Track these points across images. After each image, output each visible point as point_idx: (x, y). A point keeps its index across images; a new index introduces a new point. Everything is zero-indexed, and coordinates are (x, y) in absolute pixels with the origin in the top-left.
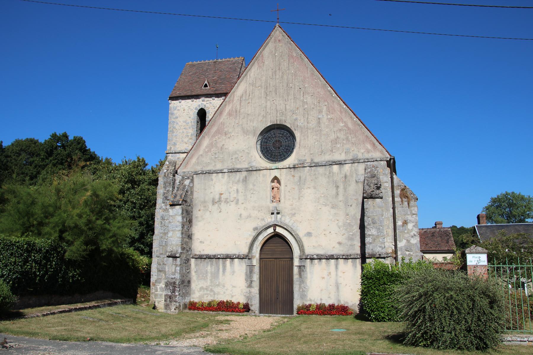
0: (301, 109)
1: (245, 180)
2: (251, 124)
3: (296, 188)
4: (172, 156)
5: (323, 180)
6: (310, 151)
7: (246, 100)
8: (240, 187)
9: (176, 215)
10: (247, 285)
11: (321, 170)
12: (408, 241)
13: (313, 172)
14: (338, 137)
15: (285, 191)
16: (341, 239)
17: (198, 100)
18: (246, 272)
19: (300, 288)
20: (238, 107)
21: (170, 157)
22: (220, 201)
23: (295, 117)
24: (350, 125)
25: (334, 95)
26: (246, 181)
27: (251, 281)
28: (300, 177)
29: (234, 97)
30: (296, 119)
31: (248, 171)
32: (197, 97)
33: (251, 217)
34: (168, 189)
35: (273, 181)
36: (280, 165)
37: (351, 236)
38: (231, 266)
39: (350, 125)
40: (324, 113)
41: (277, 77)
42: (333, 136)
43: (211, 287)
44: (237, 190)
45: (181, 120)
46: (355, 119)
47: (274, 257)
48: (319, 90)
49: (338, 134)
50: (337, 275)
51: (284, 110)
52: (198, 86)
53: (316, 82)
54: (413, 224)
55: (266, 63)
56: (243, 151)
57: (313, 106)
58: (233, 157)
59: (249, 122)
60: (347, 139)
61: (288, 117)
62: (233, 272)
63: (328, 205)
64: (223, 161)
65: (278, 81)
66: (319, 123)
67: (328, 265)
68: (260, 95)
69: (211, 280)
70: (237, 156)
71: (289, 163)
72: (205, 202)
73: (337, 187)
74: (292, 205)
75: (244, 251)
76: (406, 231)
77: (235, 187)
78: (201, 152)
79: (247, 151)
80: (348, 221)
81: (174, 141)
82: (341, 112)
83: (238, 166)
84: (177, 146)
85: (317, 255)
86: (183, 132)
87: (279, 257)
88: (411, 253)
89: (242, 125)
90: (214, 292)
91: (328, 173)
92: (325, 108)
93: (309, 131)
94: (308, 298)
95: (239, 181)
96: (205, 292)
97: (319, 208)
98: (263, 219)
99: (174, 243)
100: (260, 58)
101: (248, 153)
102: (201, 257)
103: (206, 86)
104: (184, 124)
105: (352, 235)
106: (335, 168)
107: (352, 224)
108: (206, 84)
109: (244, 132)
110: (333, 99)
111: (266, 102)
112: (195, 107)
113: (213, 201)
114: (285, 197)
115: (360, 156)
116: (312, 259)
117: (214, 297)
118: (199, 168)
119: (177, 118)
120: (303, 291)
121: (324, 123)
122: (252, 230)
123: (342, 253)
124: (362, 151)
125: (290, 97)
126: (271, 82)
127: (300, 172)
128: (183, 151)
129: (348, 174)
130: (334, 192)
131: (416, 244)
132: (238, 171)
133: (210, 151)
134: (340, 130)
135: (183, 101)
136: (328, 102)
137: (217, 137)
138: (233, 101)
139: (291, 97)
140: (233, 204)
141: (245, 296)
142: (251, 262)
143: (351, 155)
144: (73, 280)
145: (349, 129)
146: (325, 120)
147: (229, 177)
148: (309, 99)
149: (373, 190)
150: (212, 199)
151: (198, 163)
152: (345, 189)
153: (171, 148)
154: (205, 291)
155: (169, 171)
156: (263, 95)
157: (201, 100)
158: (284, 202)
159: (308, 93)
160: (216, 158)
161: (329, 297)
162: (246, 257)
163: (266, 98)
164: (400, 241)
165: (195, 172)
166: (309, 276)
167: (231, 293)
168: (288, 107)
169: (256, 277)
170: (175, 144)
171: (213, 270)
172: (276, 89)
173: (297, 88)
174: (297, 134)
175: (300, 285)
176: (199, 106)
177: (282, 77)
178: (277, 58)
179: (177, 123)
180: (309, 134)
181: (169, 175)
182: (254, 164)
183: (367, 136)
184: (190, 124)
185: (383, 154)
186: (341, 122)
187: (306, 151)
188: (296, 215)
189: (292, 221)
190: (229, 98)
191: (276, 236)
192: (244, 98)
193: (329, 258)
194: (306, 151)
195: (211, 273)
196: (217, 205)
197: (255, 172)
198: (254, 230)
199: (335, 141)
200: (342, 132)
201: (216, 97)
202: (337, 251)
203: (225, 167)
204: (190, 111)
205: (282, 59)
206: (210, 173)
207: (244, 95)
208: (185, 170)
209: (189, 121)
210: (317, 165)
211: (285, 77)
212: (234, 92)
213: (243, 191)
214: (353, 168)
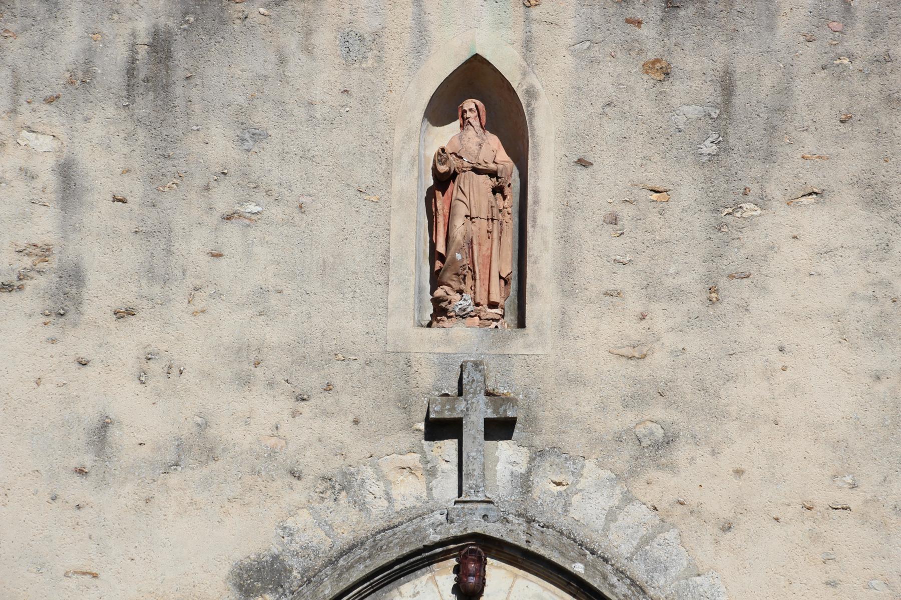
3: (688, 189)
8: (102, 142)
15: (567, 211)
28: (727, 86)
33: (210, 454)
35: (443, 108)
44: (67, 174)
77: (44, 143)
95: (83, 79)
98: (340, 484)
114: (567, 270)
127: (732, 35)
158: (563, 323)
188: (681, 453)
189: (638, 512)
213: (134, 188)
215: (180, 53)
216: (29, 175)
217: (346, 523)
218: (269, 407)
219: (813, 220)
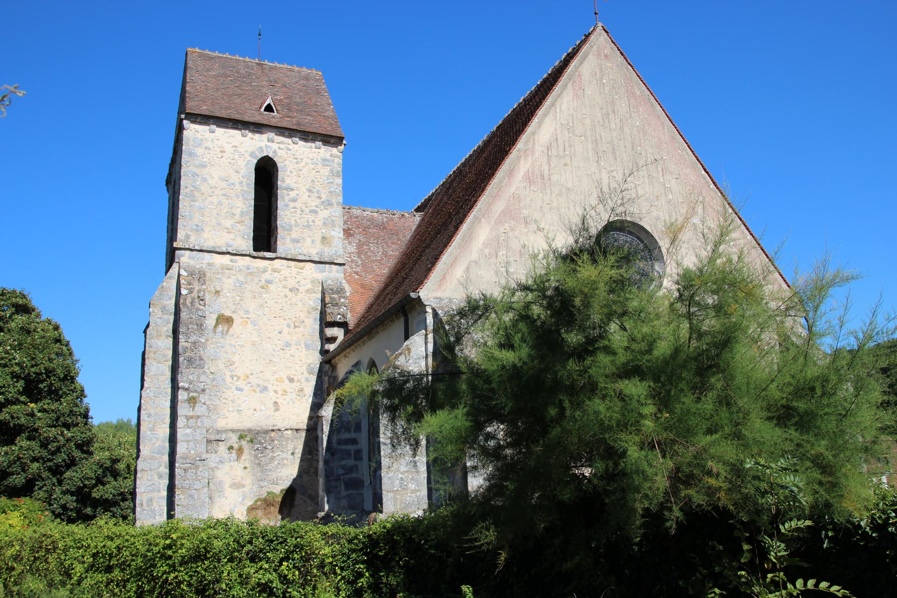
4: (190, 258)
17: (257, 136)
20: (545, 167)
25: (712, 186)
29: (534, 144)
32: (257, 127)
41: (613, 126)
55: (588, 92)
68: (585, 154)
78: (474, 255)
84: (206, 235)
104: (224, 184)
111: (600, 172)
112: (250, 150)
119: (205, 166)
126: (603, 134)
128: (224, 250)
135: (220, 131)
137: (507, 226)
138: (533, 152)
153: (188, 237)
156: (591, 155)
157: (265, 137)
159: (671, 173)
163: (597, 162)
170: (199, 230)
177: (621, 129)
178: (607, 89)
179: (205, 180)
201: (301, 139)
204: (237, 157)
207: (554, 145)
208: (439, 294)
209: (235, 178)
211: (627, 130)
212: (534, 133)
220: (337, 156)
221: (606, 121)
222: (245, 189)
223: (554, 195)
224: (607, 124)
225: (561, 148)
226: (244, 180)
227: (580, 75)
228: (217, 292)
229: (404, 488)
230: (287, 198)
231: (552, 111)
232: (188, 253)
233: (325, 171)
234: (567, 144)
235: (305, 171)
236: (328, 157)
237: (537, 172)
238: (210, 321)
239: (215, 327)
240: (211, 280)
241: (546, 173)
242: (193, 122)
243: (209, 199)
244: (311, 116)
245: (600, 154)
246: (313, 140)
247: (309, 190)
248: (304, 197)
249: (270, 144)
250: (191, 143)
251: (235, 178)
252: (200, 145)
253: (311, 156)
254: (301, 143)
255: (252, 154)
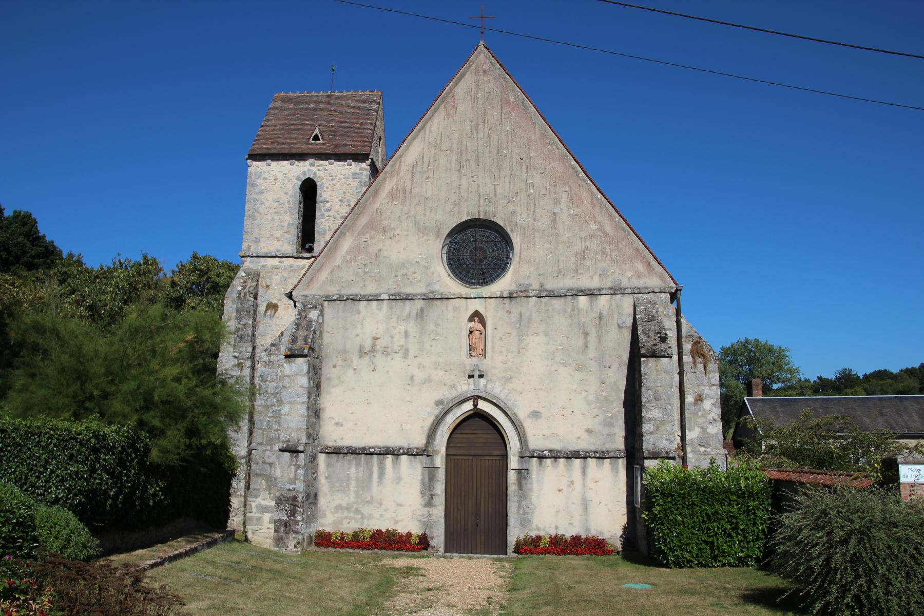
0: (522, 196)
1: (421, 315)
2: (432, 215)
3: (514, 333)
5: (562, 322)
6: (537, 268)
7: (422, 172)
9: (297, 374)
10: (423, 503)
11: (557, 303)
12: (704, 430)
13: (543, 307)
14: (587, 248)
15: (493, 337)
16: (591, 423)
17: (302, 163)
18: (422, 480)
19: (519, 507)
20: (408, 183)
21: (248, 263)
22: (373, 350)
23: (511, 208)
24: (608, 229)
25: (582, 174)
26: (422, 317)
27: (432, 496)
28: (521, 315)
29: (400, 165)
30: (513, 213)
31: (427, 298)
32: (301, 157)
33: (430, 381)
34: (244, 321)
35: (471, 319)
36: (485, 291)
37: (609, 420)
38: (394, 467)
39: (608, 229)
40: (563, 205)
41: (481, 135)
42: (578, 246)
43: (355, 506)
45: (269, 198)
46: (618, 219)
47: (472, 452)
48: (556, 164)
49: (588, 244)
50: (584, 485)
51: (492, 195)
52: (300, 138)
53: (549, 150)
54: (712, 401)
56: (418, 262)
57: (544, 192)
58: (399, 274)
59: (428, 212)
60: (603, 252)
61: (500, 208)
62: (398, 479)
63: (570, 365)
64: (378, 279)
65: (481, 142)
66: (554, 221)
67: (569, 468)
68: (448, 166)
69: (356, 492)
70: (405, 271)
71: (500, 289)
72: (344, 351)
73: (586, 334)
74: (505, 363)
75: (419, 441)
76: (700, 413)
77: (402, 327)
78: (338, 261)
79: (424, 263)
80: (604, 394)
81: (255, 235)
82: (593, 206)
83: (408, 290)
84: (262, 244)
85: (550, 451)
86: (273, 220)
87: (480, 452)
88: (709, 450)
89: (415, 217)
90: (362, 514)
91: (569, 310)
92: (565, 196)
93: (537, 234)
94: (534, 526)
95: (409, 316)
96: (346, 514)
97: (553, 369)
98: (453, 386)
99: (293, 425)
100: (449, 100)
101: (427, 268)
102: (337, 452)
103: (316, 138)
104: (276, 204)
105: (611, 417)
106: (583, 301)
107: (611, 398)
108: (316, 135)
109: (419, 230)
110: (580, 182)
111: (460, 179)
113: (360, 351)
114: (493, 348)
115: (625, 283)
116: (541, 458)
117: (362, 523)
118: (333, 290)
119: (263, 193)
120: (525, 513)
121: (564, 223)
122: (432, 404)
123: (593, 448)
124: (629, 274)
125: (503, 173)
126: (469, 145)
128: (274, 254)
129: (605, 313)
130: (580, 343)
131: (716, 434)
132: (408, 298)
133: (354, 259)
134: (592, 236)
135: (274, 164)
136: (569, 186)
137: (367, 236)
139: (505, 172)
140: (398, 358)
141: (420, 521)
142: (432, 461)
143: (610, 279)
144: (154, 502)
145: (606, 234)
146: (564, 216)
147: (391, 308)
148: (537, 179)
149: (655, 342)
150: (357, 348)
151: (331, 281)
152: (599, 338)
153: (249, 247)
154: (346, 511)
155: (247, 290)
156: (453, 165)
157: (307, 163)
158: (492, 358)
159: (536, 169)
160: (365, 273)
161: (571, 524)
162: (425, 452)
163: (459, 171)
164: (690, 430)
165: (326, 297)
166: (535, 486)
167: (394, 515)
168: (499, 190)
169: (440, 488)
170: (257, 241)
171: (361, 475)
172: (478, 156)
173: (516, 158)
174: (516, 239)
175: (519, 502)
176: (304, 173)
177: (489, 136)
178: (480, 102)
179: (262, 203)
180: (537, 240)
181: (248, 297)
182: (437, 287)
183: (637, 250)
184: (286, 205)
185: (665, 282)
186: (592, 223)
187: (532, 269)
188: (513, 380)
189: (506, 391)
190: (392, 166)
191: (478, 415)
192: (419, 169)
193: (572, 455)
194: (532, 269)
195: (357, 480)
196: (367, 358)
197: (439, 303)
198: (437, 405)
199: (583, 254)
200: (594, 240)
202: (584, 444)
203: (383, 291)
204: (286, 182)
205: (490, 104)
206: (354, 299)
207: (420, 163)
209: (285, 199)
210: (551, 295)
212: (401, 156)
213: (417, 335)
214: (613, 302)
215: (425, 311)
216: (400, 333)
217: (454, 393)
218: (441, 373)
219: (536, 339)
220: (365, 169)
221: (475, 132)
222: (292, 205)
223: (412, 205)
224: (475, 135)
225: (426, 164)
226: (291, 199)
227: (454, 96)
228: (268, 286)
229: (270, 428)
230: (323, 209)
231: (421, 134)
232: (249, 259)
233: (355, 183)
234: (432, 160)
235: (338, 185)
236: (358, 171)
237: (400, 188)
238: (262, 308)
239: (266, 312)
240: (263, 278)
241: (408, 187)
242: (255, 160)
243: (265, 217)
244: (349, 137)
245: (464, 163)
246: (345, 160)
247: (341, 201)
248: (337, 207)
249: (311, 168)
250: (253, 176)
251: (285, 199)
252: (259, 177)
253: (343, 173)
254: (336, 163)
255: (298, 178)
